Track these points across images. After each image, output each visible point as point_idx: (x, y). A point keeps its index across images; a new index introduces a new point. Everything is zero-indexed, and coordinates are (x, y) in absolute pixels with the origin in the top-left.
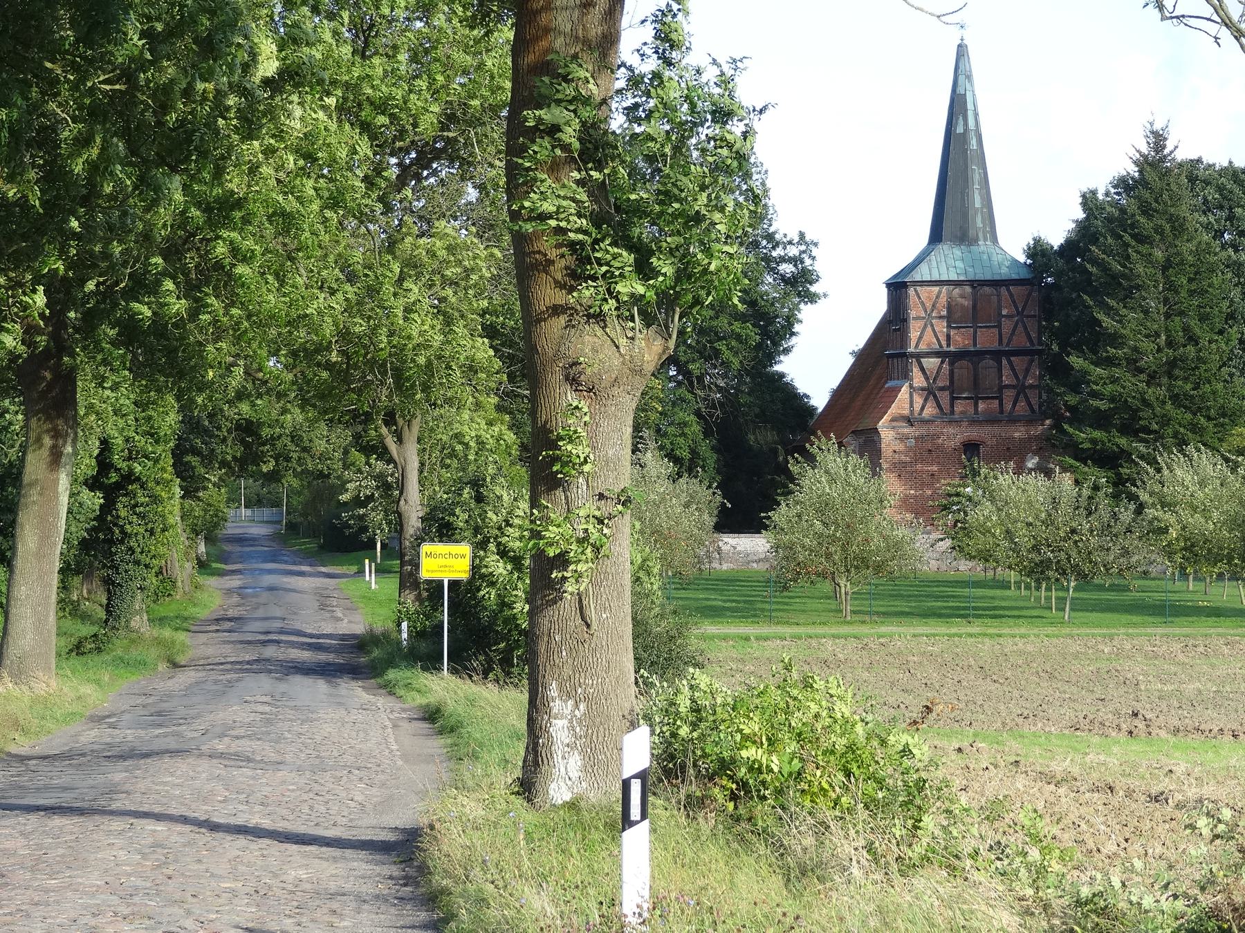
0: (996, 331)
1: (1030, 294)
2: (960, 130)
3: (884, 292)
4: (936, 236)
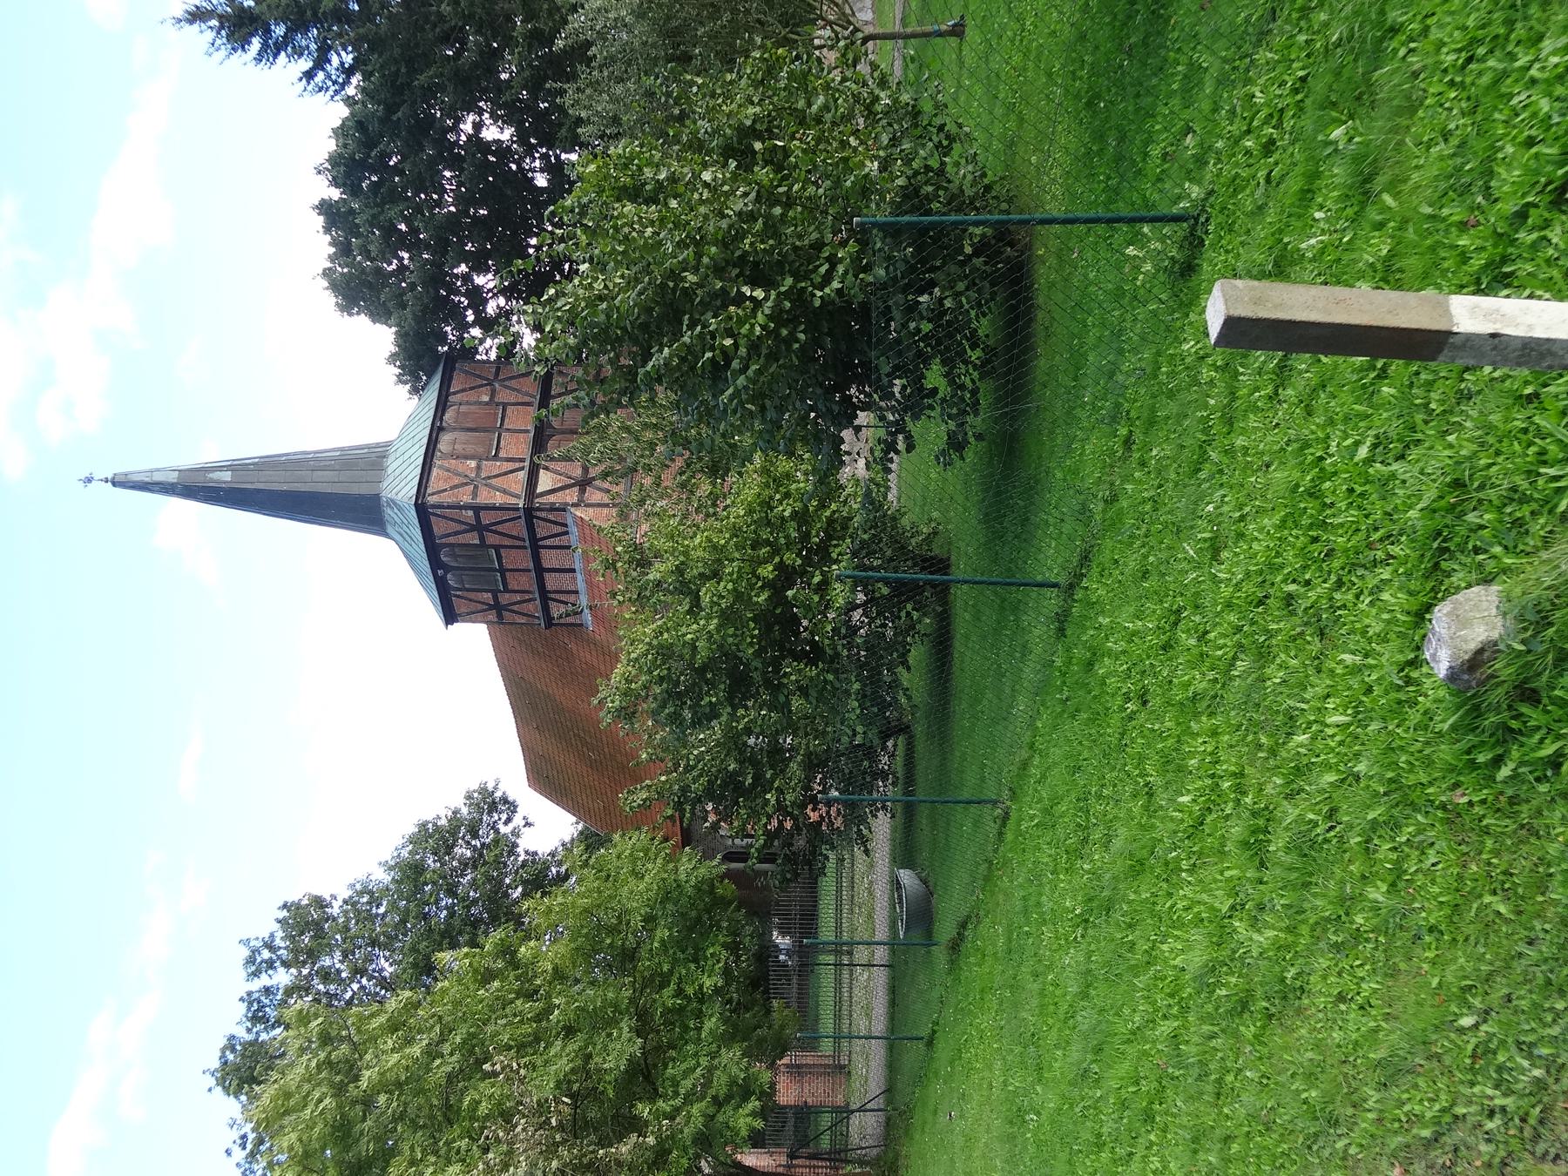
1: (467, 372)
2: (226, 476)
3: (459, 628)
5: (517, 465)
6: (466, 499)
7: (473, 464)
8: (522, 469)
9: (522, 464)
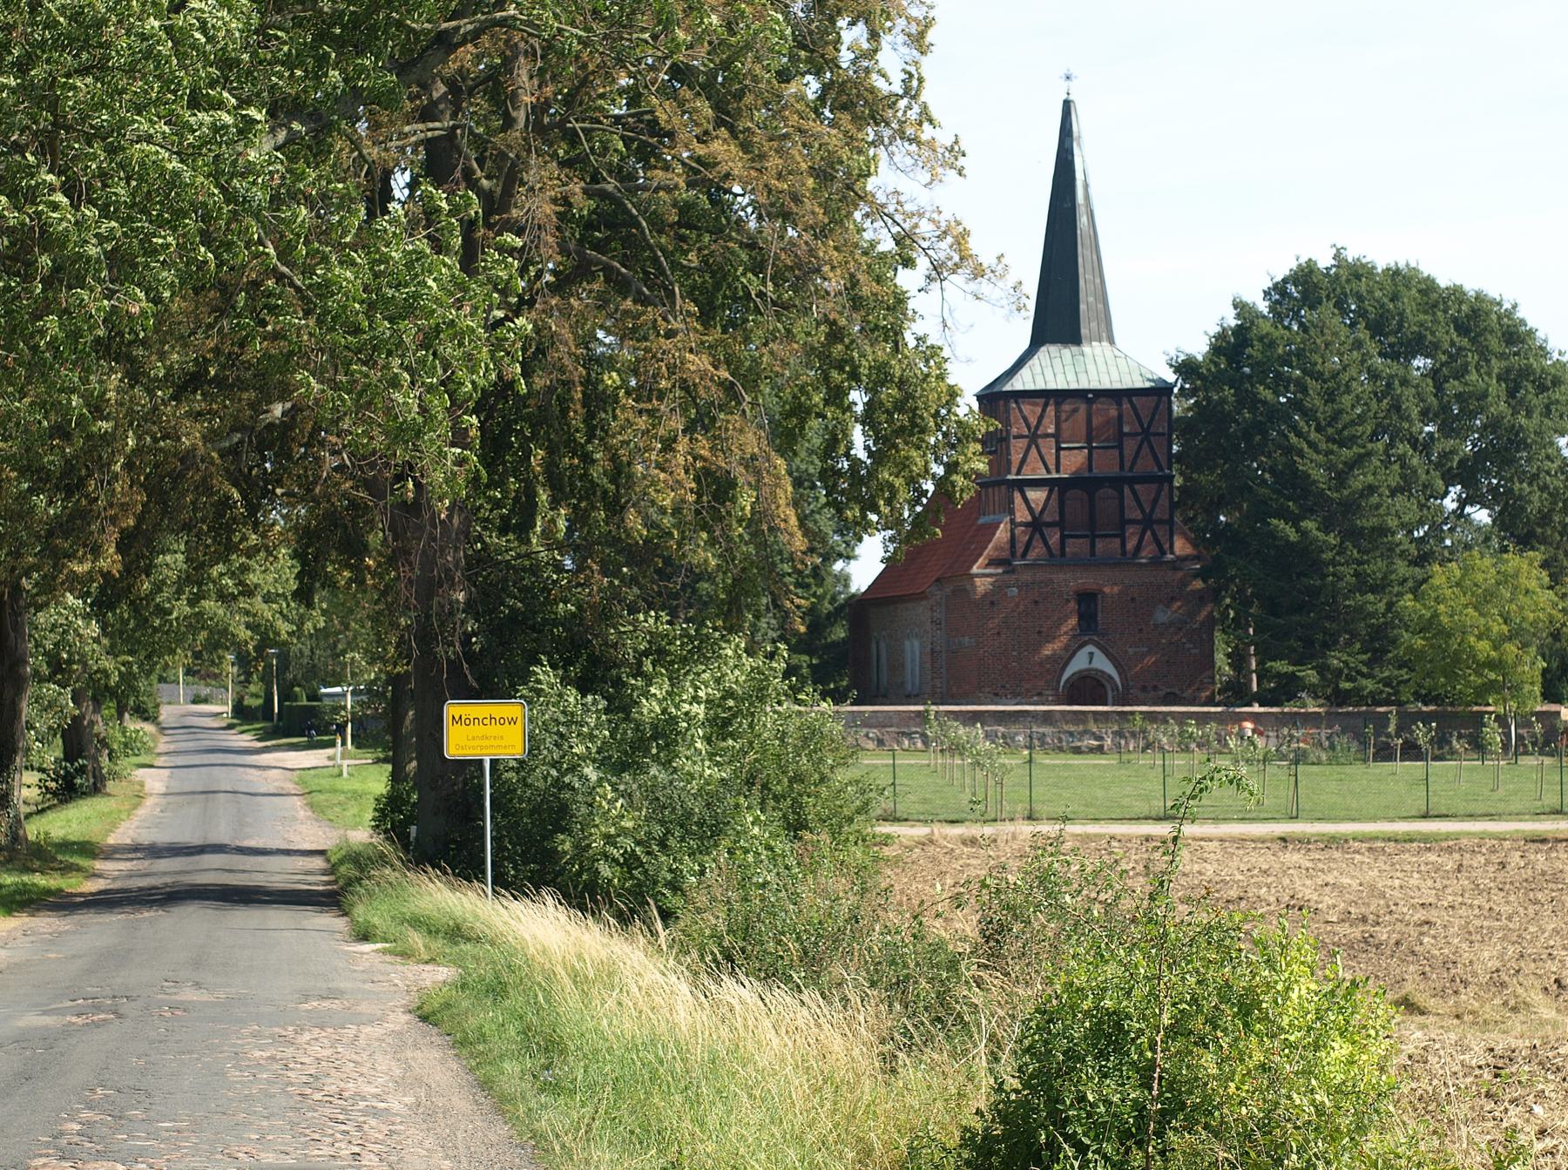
0: (1116, 452)
4: (1040, 337)
7: (1051, 430)
8: (1048, 472)
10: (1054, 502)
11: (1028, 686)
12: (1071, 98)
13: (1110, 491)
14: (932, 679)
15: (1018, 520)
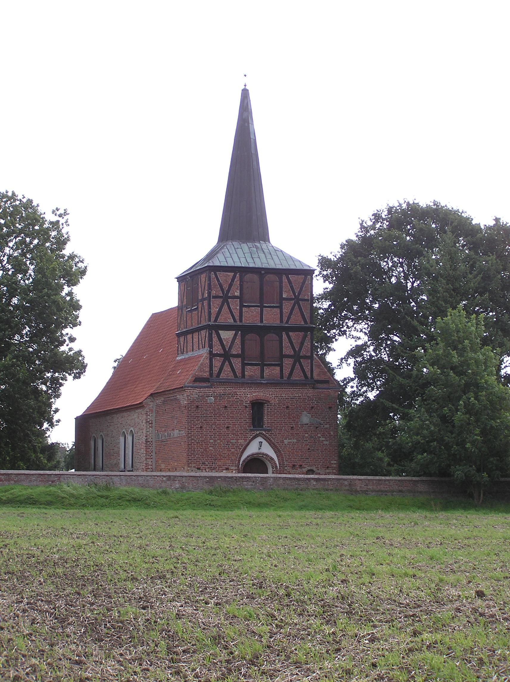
0: (278, 310)
3: (175, 285)
5: (237, 318)
6: (214, 293)
7: (237, 294)
8: (235, 320)
9: (238, 321)
10: (238, 341)
11: (220, 463)
12: (247, 87)
13: (274, 335)
14: (146, 459)
15: (215, 352)
